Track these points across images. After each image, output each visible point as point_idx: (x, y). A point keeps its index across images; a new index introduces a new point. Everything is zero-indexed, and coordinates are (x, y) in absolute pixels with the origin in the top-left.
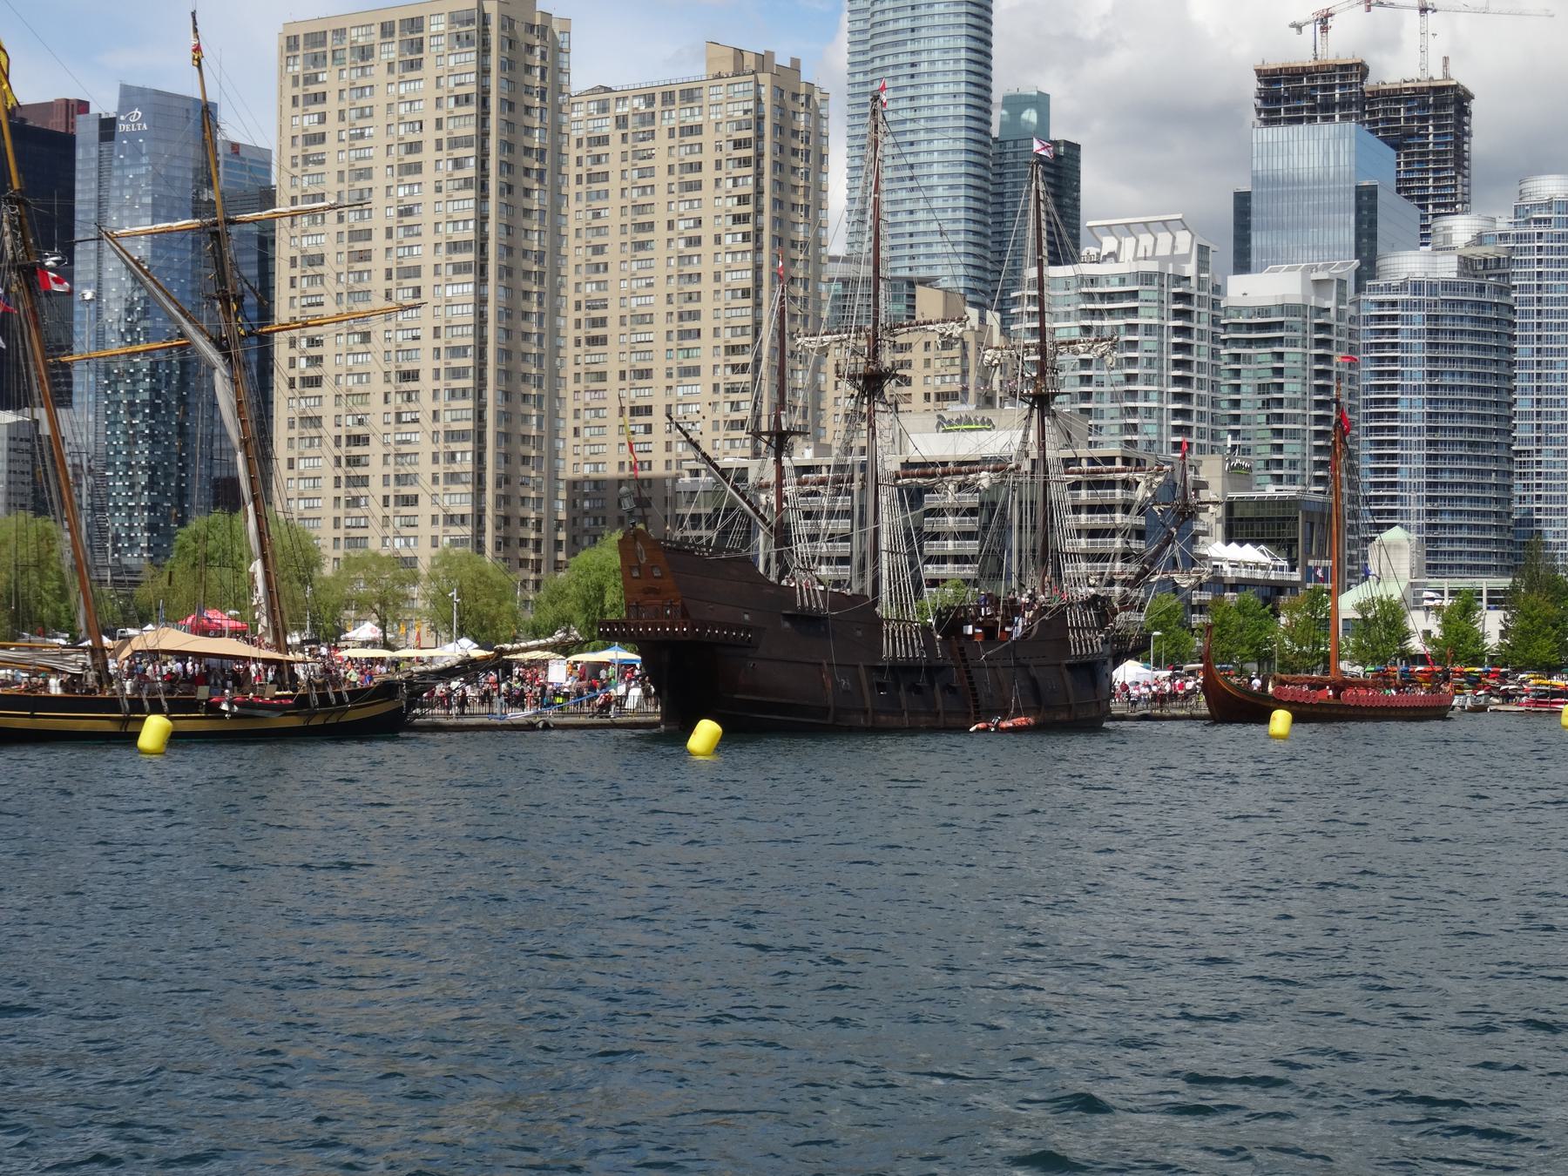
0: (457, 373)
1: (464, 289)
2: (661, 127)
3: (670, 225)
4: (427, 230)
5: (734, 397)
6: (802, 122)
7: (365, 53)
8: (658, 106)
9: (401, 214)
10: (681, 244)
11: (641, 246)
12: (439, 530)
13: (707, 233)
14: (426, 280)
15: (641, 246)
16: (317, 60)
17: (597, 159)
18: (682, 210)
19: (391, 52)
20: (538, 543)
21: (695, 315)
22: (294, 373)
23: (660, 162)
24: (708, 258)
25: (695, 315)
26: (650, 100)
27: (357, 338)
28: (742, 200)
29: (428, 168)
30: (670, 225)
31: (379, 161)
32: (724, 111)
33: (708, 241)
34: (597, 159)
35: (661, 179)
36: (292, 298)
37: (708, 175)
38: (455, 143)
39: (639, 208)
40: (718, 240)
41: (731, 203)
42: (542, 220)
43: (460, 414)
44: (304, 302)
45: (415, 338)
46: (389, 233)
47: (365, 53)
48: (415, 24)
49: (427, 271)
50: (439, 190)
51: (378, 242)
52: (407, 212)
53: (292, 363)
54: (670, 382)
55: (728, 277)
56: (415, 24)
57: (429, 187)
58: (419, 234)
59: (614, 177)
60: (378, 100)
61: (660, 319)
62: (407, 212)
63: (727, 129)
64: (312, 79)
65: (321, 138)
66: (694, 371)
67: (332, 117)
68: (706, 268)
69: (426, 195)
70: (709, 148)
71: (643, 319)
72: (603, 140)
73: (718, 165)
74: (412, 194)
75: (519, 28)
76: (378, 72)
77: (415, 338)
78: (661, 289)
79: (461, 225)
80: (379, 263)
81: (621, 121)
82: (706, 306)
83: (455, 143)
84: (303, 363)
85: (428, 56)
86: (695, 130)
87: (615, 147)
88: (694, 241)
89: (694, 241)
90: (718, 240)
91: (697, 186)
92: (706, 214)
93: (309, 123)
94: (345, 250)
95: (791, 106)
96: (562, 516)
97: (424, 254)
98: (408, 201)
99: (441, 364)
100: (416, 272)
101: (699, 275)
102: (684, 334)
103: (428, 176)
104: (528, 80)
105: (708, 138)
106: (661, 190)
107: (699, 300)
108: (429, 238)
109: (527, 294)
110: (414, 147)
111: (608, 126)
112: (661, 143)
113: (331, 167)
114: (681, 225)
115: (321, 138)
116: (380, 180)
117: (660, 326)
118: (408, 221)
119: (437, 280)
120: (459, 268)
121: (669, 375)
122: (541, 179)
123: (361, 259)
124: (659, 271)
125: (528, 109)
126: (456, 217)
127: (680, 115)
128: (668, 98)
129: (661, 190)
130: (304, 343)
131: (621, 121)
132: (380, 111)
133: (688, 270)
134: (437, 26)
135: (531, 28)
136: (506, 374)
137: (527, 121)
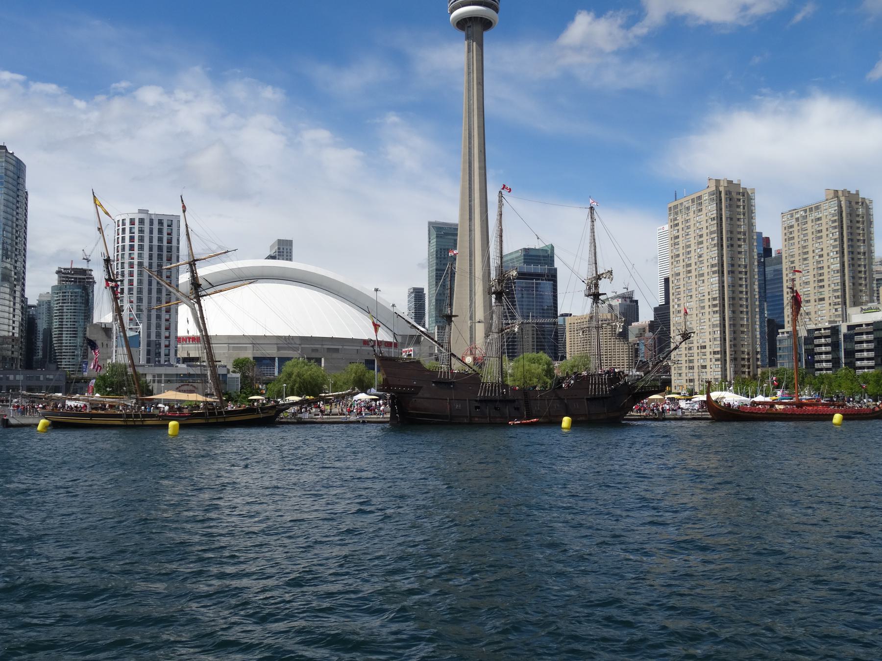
0: (715, 306)
1: (715, 279)
2: (809, 219)
3: (813, 251)
4: (705, 261)
5: (836, 307)
6: (861, 211)
7: (688, 208)
8: (808, 213)
10: (817, 257)
11: (805, 259)
12: (712, 356)
13: (825, 253)
15: (805, 259)
16: (677, 213)
17: (791, 233)
19: (694, 208)
20: (749, 360)
23: (809, 231)
24: (825, 261)
25: (822, 280)
26: (805, 211)
28: (835, 240)
29: (705, 242)
30: (813, 251)
31: (693, 242)
32: (829, 211)
34: (791, 233)
35: (810, 237)
37: (824, 233)
38: (711, 233)
39: (804, 247)
40: (828, 255)
41: (832, 241)
42: (745, 255)
43: (716, 319)
47: (688, 208)
48: (700, 198)
49: (706, 274)
55: (832, 267)
56: (700, 198)
57: (705, 248)
59: (796, 238)
60: (691, 223)
61: (812, 283)
62: (700, 256)
63: (829, 217)
64: (675, 219)
65: (677, 237)
66: (822, 299)
67: (680, 230)
68: (825, 264)
69: (705, 251)
70: (824, 224)
71: (807, 283)
72: (792, 227)
73: (827, 229)
75: (734, 194)
76: (691, 214)
78: (812, 273)
80: (694, 273)
81: (797, 219)
82: (825, 277)
83: (711, 233)
85: (703, 207)
86: (819, 219)
87: (796, 228)
88: (821, 256)
89: (821, 256)
90: (828, 255)
91: (821, 237)
92: (824, 246)
93: (675, 233)
95: (855, 206)
96: (759, 350)
97: (705, 270)
103: (705, 245)
104: (738, 210)
105: (823, 221)
106: (810, 240)
108: (706, 264)
109: (741, 279)
110: (701, 236)
111: (793, 222)
112: (810, 224)
113: (681, 245)
115: (677, 237)
116: (693, 248)
117: (812, 285)
120: (714, 272)
122: (744, 241)
124: (811, 267)
125: (739, 220)
127: (815, 215)
128: (811, 210)
129: (810, 240)
131: (797, 219)
132: (692, 226)
134: (706, 197)
135: (739, 193)
136: (732, 305)
137: (738, 223)
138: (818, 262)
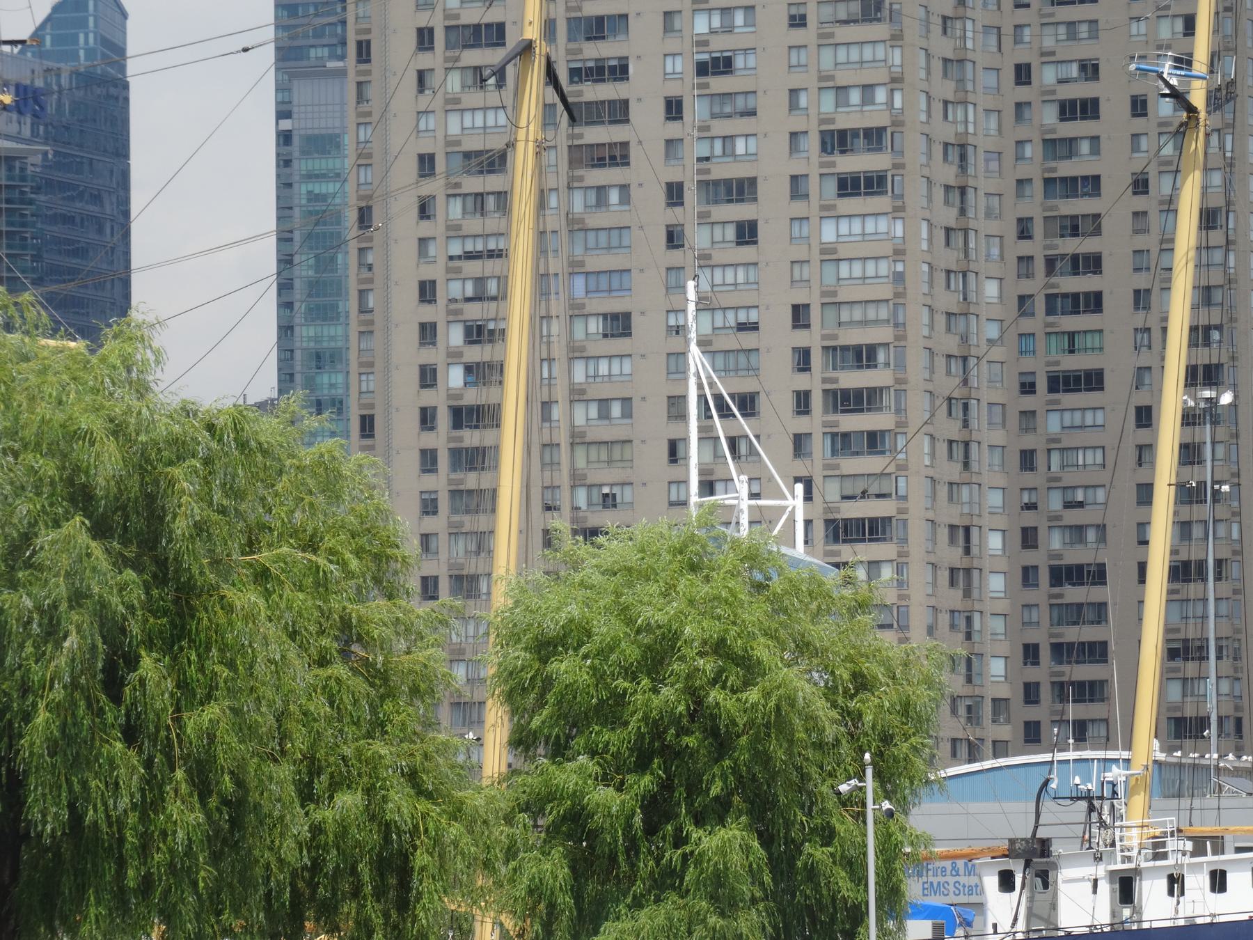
4: (772, 107)
9: (702, 69)
10: (1050, 116)
14: (771, 208)
18: (1048, 43)
21: (1093, 263)
22: (436, 398)
27: (595, 326)
33: (1115, 108)
36: (423, 242)
44: (456, 249)
45: (742, 327)
46: (674, 109)
49: (773, 191)
50: (798, 21)
51: (646, 125)
52: (723, 65)
53: (428, 377)
54: (1028, 402)
58: (752, 113)
62: (723, 65)
68: (1114, 168)
74: (729, 29)
77: (742, 327)
79: (855, 96)
80: (647, 172)
84: (456, 377)
89: (1072, 110)
94: (563, 142)
98: (720, 45)
99: (813, 382)
100: (743, 190)
101: (1096, 179)
102: (1060, 303)
107: (1097, 231)
108: (774, 118)
114: (1047, 76)
118: (719, 84)
119: (799, 208)
121: (1028, 388)
123: (600, 163)
126: (842, 79)
130: (456, 336)
133: (1066, 169)
138: (1059, 147)
